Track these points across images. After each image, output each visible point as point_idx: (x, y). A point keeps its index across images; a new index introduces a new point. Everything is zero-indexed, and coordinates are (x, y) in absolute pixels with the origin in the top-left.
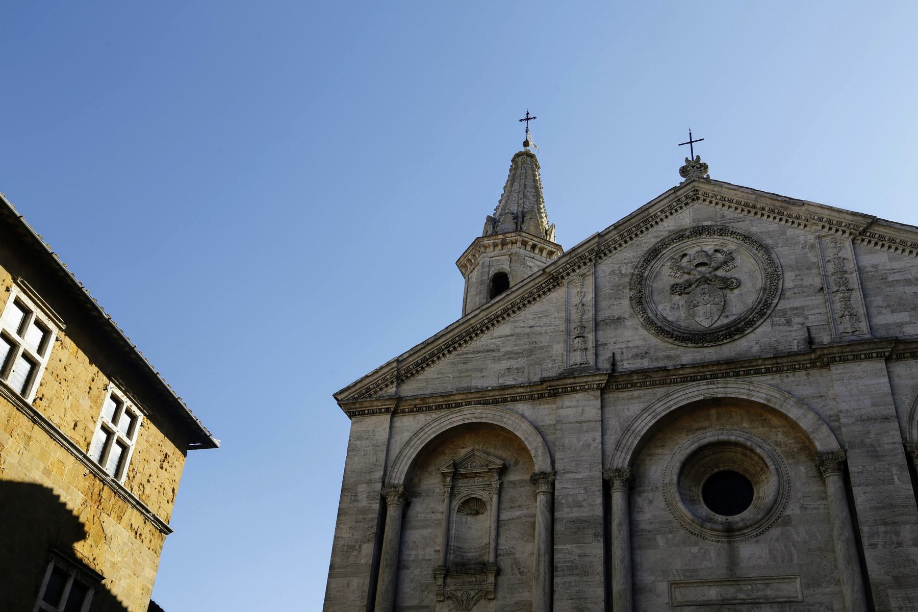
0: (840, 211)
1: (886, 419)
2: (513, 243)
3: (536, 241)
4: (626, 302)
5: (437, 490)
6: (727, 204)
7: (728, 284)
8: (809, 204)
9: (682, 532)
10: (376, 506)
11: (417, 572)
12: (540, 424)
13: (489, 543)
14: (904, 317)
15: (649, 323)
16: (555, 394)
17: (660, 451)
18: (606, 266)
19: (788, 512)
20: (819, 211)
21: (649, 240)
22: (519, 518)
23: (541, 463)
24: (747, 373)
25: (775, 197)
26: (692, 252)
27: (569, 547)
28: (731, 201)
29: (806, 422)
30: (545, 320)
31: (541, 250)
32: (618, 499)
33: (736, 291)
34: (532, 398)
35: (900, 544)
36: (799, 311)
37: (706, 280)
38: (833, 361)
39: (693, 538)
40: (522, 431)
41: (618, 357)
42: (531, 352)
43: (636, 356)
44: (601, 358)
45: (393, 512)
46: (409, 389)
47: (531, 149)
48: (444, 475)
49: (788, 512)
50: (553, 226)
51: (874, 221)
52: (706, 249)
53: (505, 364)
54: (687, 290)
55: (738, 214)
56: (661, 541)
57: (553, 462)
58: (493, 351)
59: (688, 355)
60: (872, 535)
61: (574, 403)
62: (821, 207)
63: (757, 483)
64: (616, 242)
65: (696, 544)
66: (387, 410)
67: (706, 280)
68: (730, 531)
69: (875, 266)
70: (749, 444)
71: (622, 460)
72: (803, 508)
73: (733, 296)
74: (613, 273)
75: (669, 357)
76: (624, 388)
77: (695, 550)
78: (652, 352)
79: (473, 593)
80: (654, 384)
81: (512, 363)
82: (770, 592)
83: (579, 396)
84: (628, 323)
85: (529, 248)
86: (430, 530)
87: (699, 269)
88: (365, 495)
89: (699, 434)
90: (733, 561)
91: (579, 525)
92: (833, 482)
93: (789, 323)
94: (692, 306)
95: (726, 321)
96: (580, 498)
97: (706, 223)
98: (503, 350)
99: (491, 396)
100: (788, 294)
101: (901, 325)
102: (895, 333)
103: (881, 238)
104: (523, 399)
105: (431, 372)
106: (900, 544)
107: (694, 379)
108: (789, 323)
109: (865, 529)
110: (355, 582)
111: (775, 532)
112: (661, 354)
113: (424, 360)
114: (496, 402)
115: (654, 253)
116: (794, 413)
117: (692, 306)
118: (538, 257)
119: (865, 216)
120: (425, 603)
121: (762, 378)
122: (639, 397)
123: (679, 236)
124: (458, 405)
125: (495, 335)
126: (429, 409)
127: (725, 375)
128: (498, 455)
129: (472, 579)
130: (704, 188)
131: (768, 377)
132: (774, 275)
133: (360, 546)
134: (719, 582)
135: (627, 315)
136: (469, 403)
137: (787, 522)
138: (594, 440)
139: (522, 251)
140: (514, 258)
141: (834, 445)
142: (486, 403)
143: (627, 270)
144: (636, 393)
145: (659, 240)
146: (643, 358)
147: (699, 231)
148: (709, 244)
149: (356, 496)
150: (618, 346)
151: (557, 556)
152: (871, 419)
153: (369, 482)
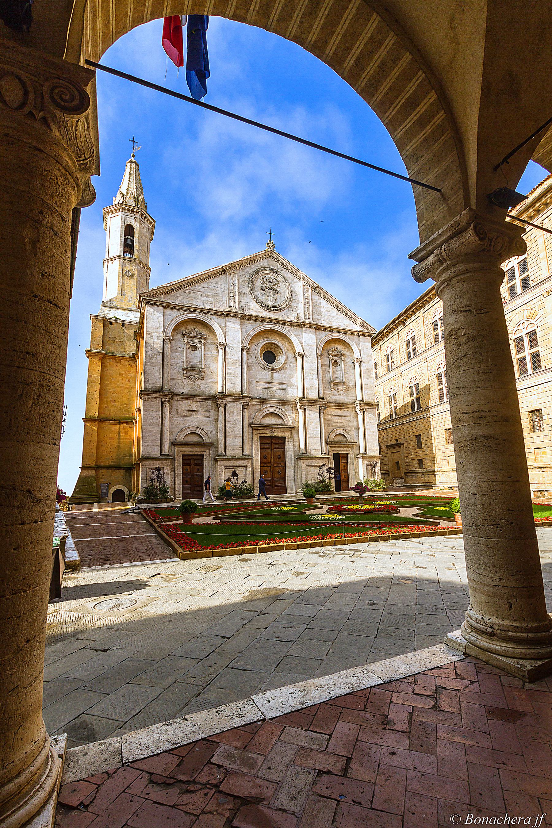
5: (180, 340)
6: (279, 263)
7: (277, 292)
9: (260, 367)
11: (175, 367)
13: (201, 362)
18: (240, 272)
23: (221, 339)
30: (219, 286)
31: (147, 221)
32: (245, 355)
37: (270, 288)
38: (304, 327)
41: (244, 308)
48: (184, 335)
51: (318, 287)
52: (271, 277)
54: (265, 290)
55: (281, 267)
59: (265, 314)
61: (232, 321)
64: (245, 263)
65: (263, 371)
66: (163, 306)
67: (272, 289)
70: (279, 345)
76: (248, 319)
77: (263, 373)
78: (255, 308)
79: (196, 377)
80: (256, 321)
81: (208, 299)
87: (270, 283)
97: (272, 267)
103: (318, 292)
104: (214, 315)
105: (177, 293)
107: (268, 322)
110: (156, 369)
111: (283, 371)
112: (257, 310)
114: (205, 313)
115: (257, 272)
123: (264, 269)
124: (190, 311)
126: (179, 309)
128: (205, 333)
135: (247, 293)
136: (195, 311)
137: (286, 369)
145: (258, 268)
147: (271, 270)
148: (272, 276)
150: (244, 303)
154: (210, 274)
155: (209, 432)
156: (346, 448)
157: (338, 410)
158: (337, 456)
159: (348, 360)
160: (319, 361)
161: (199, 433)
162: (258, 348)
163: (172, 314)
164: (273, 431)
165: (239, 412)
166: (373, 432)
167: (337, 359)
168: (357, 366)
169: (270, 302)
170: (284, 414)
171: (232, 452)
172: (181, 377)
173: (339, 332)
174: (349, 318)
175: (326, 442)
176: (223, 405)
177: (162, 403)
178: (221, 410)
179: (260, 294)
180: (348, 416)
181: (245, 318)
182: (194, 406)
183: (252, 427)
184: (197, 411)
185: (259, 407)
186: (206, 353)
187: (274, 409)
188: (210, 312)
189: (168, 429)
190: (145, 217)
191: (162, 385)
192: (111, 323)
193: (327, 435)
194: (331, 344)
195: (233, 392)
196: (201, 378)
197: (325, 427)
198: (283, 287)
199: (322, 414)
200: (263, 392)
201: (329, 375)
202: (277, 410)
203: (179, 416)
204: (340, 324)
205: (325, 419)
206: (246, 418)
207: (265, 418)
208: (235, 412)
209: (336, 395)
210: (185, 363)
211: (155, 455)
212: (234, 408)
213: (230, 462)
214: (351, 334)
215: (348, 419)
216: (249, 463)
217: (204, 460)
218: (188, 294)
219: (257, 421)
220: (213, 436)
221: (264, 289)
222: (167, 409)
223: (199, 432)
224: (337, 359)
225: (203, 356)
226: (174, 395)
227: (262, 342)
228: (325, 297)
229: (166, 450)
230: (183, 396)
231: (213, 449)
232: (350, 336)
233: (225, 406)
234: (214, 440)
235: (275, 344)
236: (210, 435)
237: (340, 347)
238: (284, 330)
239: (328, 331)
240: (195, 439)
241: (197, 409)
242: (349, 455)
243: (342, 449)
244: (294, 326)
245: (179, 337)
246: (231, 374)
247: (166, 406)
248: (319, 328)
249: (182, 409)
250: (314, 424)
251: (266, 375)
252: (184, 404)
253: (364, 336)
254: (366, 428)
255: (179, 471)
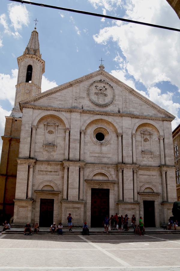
0: (128, 86)
1: (130, 129)
2: (34, 58)
3: (39, 59)
4: (86, 94)
7: (105, 95)
8: (123, 83)
9: (93, 143)
10: (31, 130)
12: (67, 117)
13: (55, 141)
14: (134, 110)
15: (90, 100)
16: (71, 112)
17: (90, 127)
19: (111, 142)
20: (125, 85)
21: (91, 81)
22: (61, 136)
23: (67, 126)
24: (108, 115)
25: (117, 79)
26: (99, 86)
27: (73, 144)
28: (108, 77)
29: (117, 127)
31: (40, 61)
32: (82, 135)
33: (107, 97)
34: (66, 112)
35: (129, 150)
36: (118, 104)
38: (123, 116)
39: (95, 145)
40: (63, 118)
41: (83, 106)
42: (65, 101)
43: (87, 107)
44: (80, 106)
45: (34, 131)
46: (37, 103)
47: (37, 30)
48: (45, 125)
49: (111, 142)
50: (41, 54)
53: (59, 102)
56: (89, 144)
57: (70, 126)
58: (56, 98)
59: (97, 109)
60: (125, 148)
61: (75, 115)
62: (125, 84)
63: (106, 136)
65: (95, 146)
66: (32, 108)
67: (102, 93)
68: (101, 144)
69: (131, 99)
70: (106, 129)
71: (83, 128)
72: (114, 142)
73: (106, 98)
74: (83, 87)
75: (93, 108)
76: (85, 113)
77: (95, 147)
80: (91, 114)
81: (60, 102)
82: (106, 156)
83: (76, 113)
84: (86, 99)
85: (38, 60)
86: (41, 136)
88: (28, 127)
89: (97, 125)
90: (101, 150)
91: (75, 140)
92: (120, 138)
93: (116, 106)
94: (98, 98)
95: (105, 103)
96: (75, 135)
98: (59, 99)
99: (57, 110)
100: (116, 100)
101: (134, 111)
102: (133, 113)
103: (133, 94)
104: (64, 111)
106: (129, 150)
107: (99, 114)
108: (116, 106)
109: (124, 147)
110: (26, 146)
112: (92, 107)
113: (40, 97)
114: (57, 111)
115: (92, 84)
116: (115, 125)
117: (98, 98)
118: (39, 63)
119: (132, 89)
120: (41, 151)
121: (110, 116)
122: (87, 116)
123: (97, 82)
124: (49, 110)
125: (57, 95)
126: (42, 109)
127: (104, 115)
129: (51, 147)
130: (103, 73)
131: (112, 117)
132: (114, 96)
133: (27, 138)
134: (98, 153)
135: (86, 97)
136: (51, 110)
138: (79, 123)
139: (36, 61)
140: (34, 62)
141: (121, 132)
142: (55, 111)
143: (86, 87)
144: (87, 115)
146: (88, 107)
148: (102, 85)
149: (25, 127)
151: (70, 146)
152: (128, 128)
153: (28, 124)
154: (62, 87)
155: (58, 185)
156: (153, 198)
157: (148, 171)
158: (146, 203)
159: (155, 137)
160: (134, 139)
161: (51, 185)
162: (91, 131)
163: (37, 112)
164: (101, 185)
165: (77, 172)
166: (173, 186)
167: (148, 137)
168: (162, 141)
169: (101, 102)
170: (109, 174)
171: (72, 198)
172: (42, 150)
173: (148, 119)
174: (156, 109)
175: (138, 193)
176: (66, 168)
177: (29, 167)
178: (66, 170)
179: (94, 98)
180: (154, 176)
181: (84, 112)
182: (49, 168)
183: (86, 182)
184: (51, 172)
185: (92, 169)
186: (57, 136)
187: (102, 170)
188: (61, 110)
189: (32, 183)
190: (39, 60)
191: (30, 155)
192: (16, 120)
193: (139, 188)
194: (143, 127)
195: (74, 159)
196: (54, 151)
197: (137, 183)
198: (109, 92)
199: (135, 174)
200: (94, 159)
201: (141, 148)
202: (104, 171)
203: (40, 174)
204: (149, 114)
205: (137, 177)
206: (81, 176)
207: (96, 176)
208: (75, 172)
209: (146, 161)
210: (45, 141)
211: (23, 198)
212: (74, 169)
213: (70, 204)
214: (157, 120)
215: (155, 177)
216: (83, 206)
217: (54, 202)
218: (49, 100)
219: (90, 178)
220: (60, 187)
221: (96, 94)
222: (31, 170)
223: (52, 185)
224: (148, 137)
225: (56, 137)
226: (37, 161)
227: (94, 127)
228: (138, 97)
229: (30, 195)
230: (42, 162)
231: (60, 196)
232: (156, 121)
233: (68, 169)
234: (61, 190)
235: (102, 128)
236: (59, 187)
237: (149, 129)
238: (110, 119)
239: (140, 118)
240: (50, 189)
241: (51, 170)
242: (155, 202)
243: (150, 198)
244: (116, 116)
245: (41, 126)
246: (73, 148)
247: (31, 168)
248: (133, 116)
249: (42, 170)
250: (129, 180)
251: (97, 148)
252: (43, 167)
253: (166, 121)
254: (168, 183)
255: (38, 209)
